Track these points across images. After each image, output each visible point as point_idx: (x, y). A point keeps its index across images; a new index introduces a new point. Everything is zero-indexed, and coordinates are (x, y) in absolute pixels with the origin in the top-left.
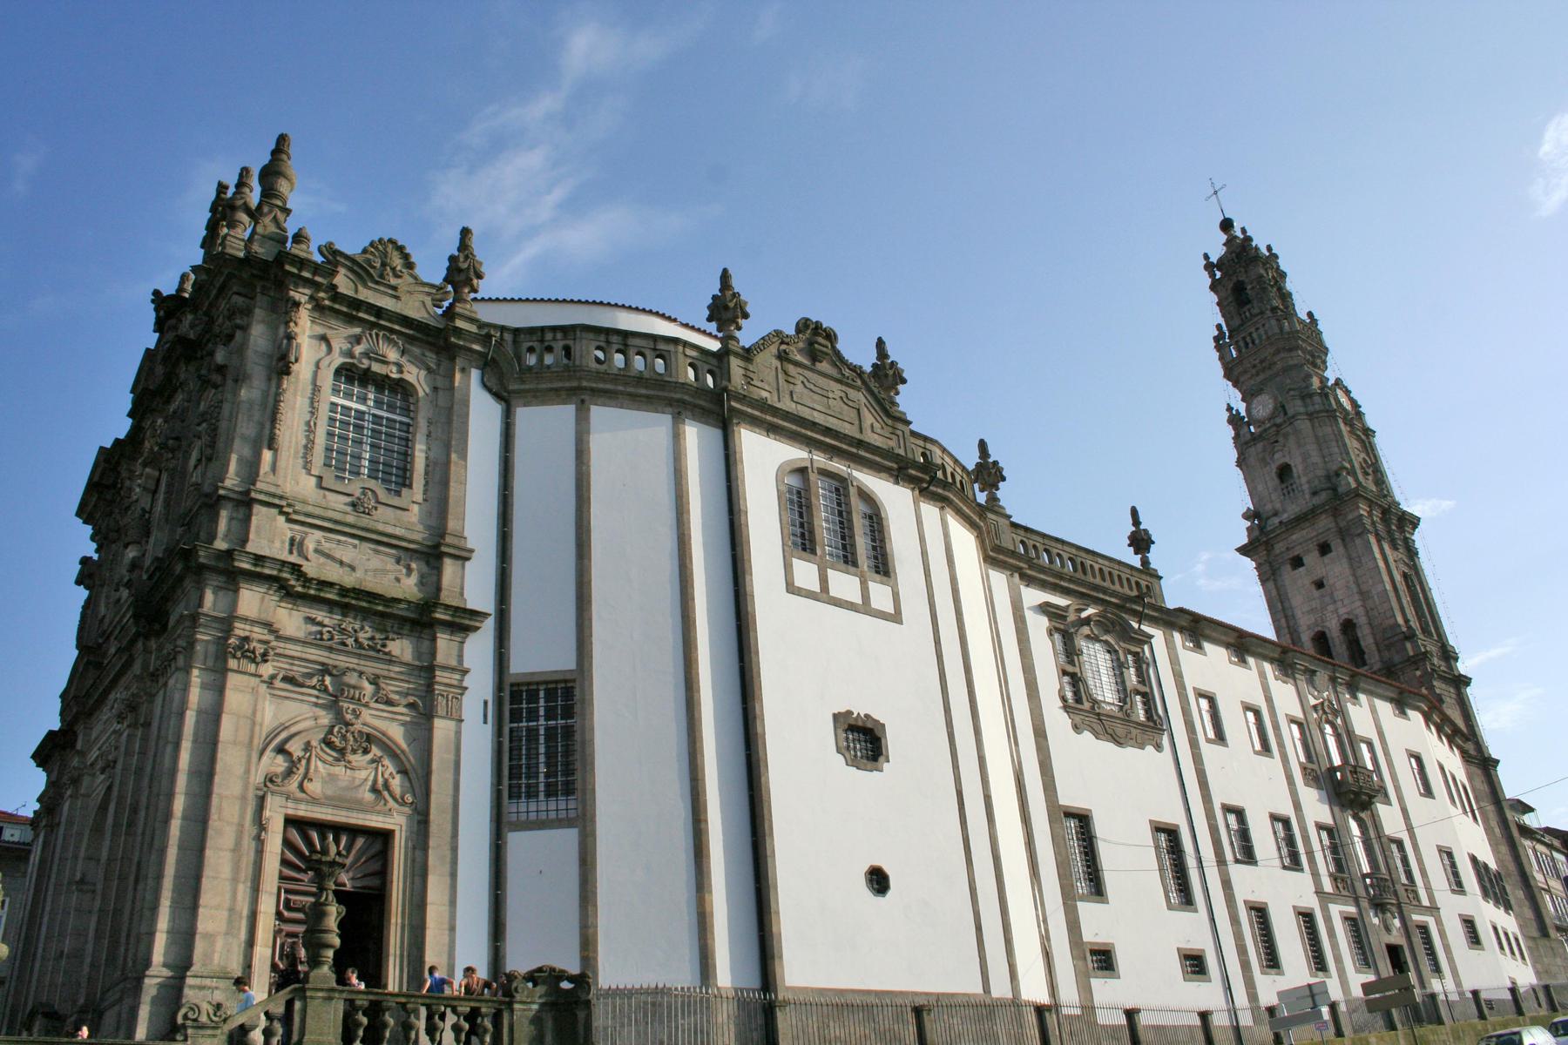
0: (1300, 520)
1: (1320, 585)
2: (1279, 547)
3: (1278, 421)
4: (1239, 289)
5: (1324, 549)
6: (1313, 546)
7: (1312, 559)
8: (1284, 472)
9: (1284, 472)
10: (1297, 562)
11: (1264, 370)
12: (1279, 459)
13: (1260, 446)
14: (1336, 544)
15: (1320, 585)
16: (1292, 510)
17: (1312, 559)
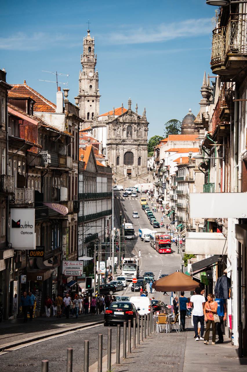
0: (91, 96)
1: (91, 106)
2: (86, 98)
3: (93, 78)
4: (90, 48)
5: (93, 101)
6: (92, 100)
7: (91, 102)
8: (91, 86)
9: (91, 86)
10: (88, 101)
11: (90, 66)
12: (91, 84)
13: (89, 80)
14: (95, 101)
15: (91, 106)
16: (90, 93)
17: (91, 102)
